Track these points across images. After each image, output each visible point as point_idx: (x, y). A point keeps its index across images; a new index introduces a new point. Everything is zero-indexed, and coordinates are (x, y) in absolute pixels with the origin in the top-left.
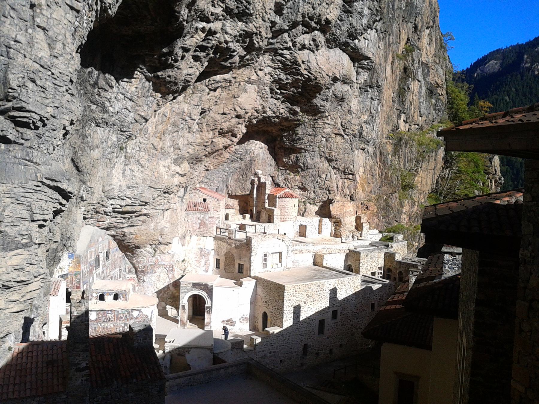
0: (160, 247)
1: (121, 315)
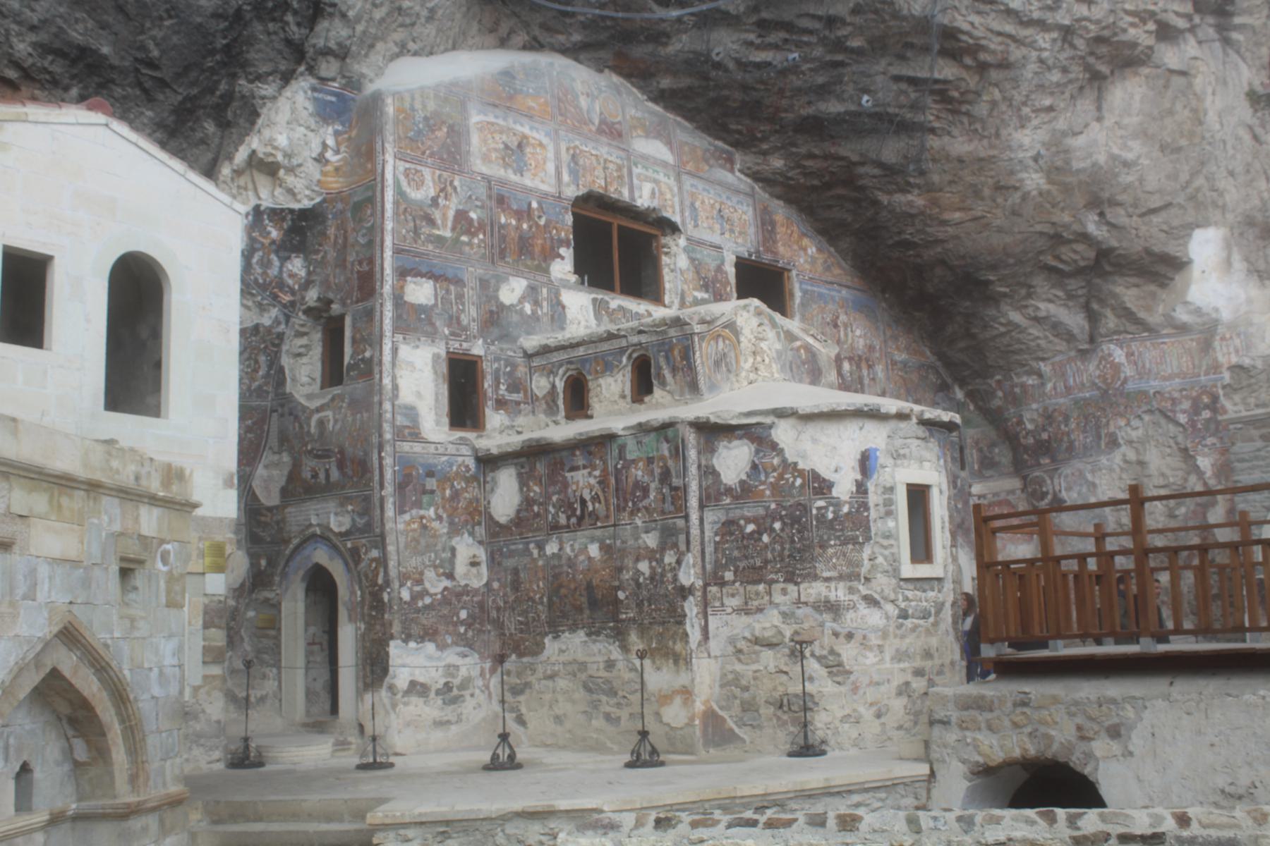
0: (1119, 290)
1: (638, 473)
